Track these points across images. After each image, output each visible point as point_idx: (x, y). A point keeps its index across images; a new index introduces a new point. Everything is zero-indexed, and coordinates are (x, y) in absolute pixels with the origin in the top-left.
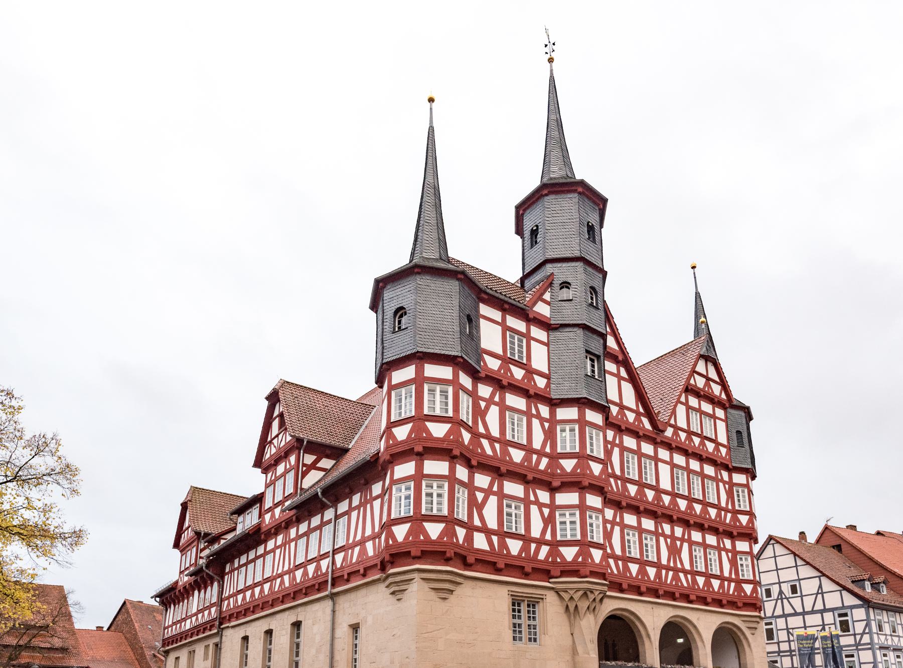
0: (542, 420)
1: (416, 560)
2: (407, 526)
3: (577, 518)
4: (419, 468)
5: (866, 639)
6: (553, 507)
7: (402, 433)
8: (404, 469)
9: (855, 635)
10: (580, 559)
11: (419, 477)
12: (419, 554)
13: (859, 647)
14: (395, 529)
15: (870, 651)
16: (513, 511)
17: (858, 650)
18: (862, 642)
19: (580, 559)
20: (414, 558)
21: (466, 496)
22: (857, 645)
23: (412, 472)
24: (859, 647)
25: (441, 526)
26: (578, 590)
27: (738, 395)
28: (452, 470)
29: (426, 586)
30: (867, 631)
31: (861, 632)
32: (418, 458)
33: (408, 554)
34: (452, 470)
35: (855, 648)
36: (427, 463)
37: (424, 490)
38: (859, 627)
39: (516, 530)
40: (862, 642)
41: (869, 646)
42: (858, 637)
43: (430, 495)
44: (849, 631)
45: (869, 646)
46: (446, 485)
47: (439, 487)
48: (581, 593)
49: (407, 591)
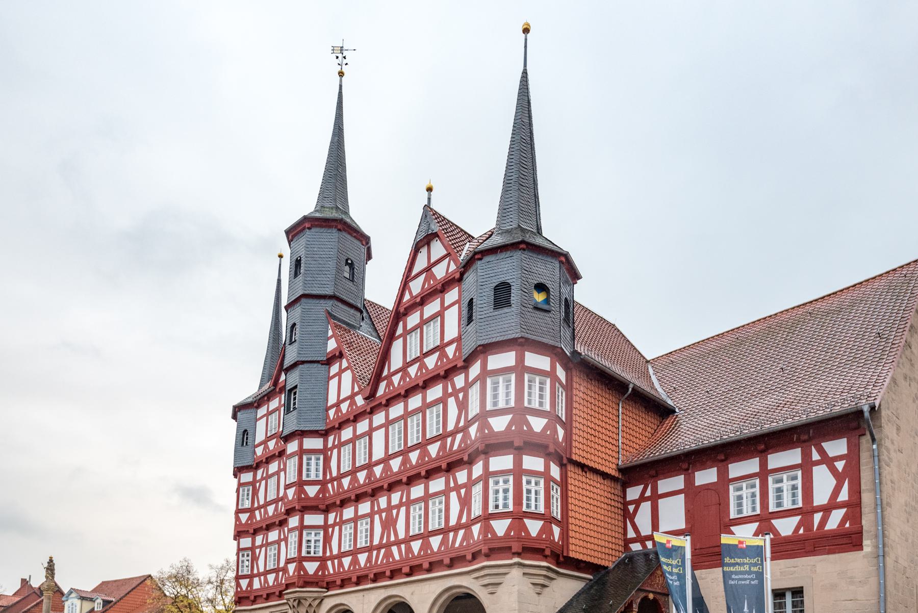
1: (516, 555)
2: (508, 522)
4: (518, 462)
8: (502, 462)
12: (520, 551)
14: (494, 524)
20: (514, 554)
21: (559, 493)
23: (510, 466)
25: (540, 524)
28: (547, 467)
29: (527, 581)
32: (516, 452)
34: (547, 467)
36: (526, 459)
37: (525, 487)
43: (529, 491)
46: (542, 481)
47: (536, 484)
49: (502, 585)
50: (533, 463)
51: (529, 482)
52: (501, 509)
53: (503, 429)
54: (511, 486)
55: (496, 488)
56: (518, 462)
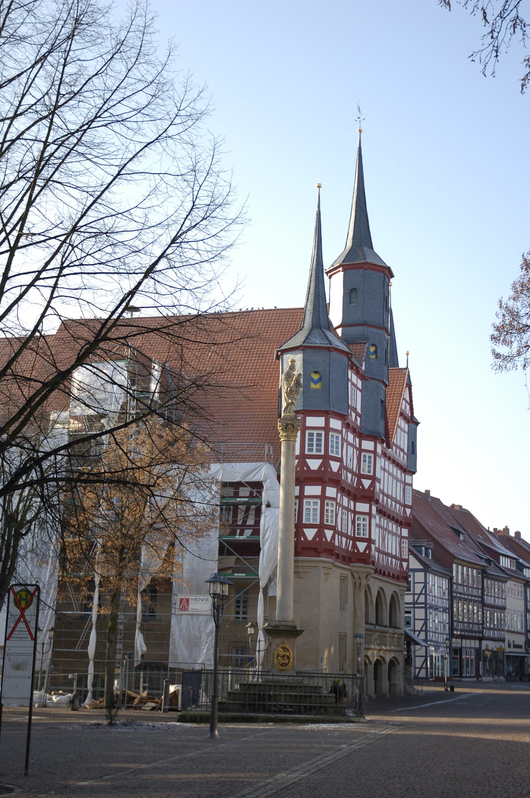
0: (357, 449)
3: (367, 523)
4: (323, 491)
5: (422, 599)
6: (355, 512)
7: (314, 464)
9: (414, 594)
10: (367, 552)
11: (323, 497)
13: (416, 606)
15: (423, 610)
16: (362, 522)
17: (415, 608)
18: (418, 601)
19: (367, 552)
22: (415, 603)
24: (416, 606)
26: (364, 572)
27: (417, 415)
30: (423, 592)
31: (419, 592)
33: (316, 549)
35: (412, 606)
37: (326, 508)
38: (418, 588)
39: (363, 535)
40: (418, 601)
41: (423, 605)
42: (416, 597)
44: (410, 591)
45: (423, 605)
48: (366, 574)
50: (331, 492)
51: (327, 505)
52: (311, 522)
53: (316, 469)
54: (318, 507)
55: (308, 507)
56: (323, 491)
